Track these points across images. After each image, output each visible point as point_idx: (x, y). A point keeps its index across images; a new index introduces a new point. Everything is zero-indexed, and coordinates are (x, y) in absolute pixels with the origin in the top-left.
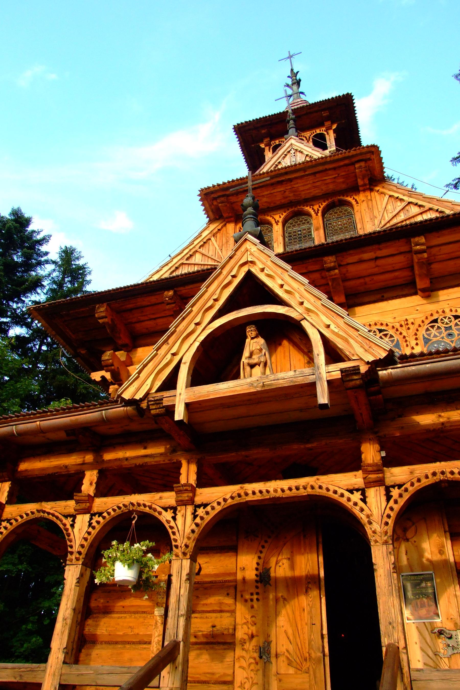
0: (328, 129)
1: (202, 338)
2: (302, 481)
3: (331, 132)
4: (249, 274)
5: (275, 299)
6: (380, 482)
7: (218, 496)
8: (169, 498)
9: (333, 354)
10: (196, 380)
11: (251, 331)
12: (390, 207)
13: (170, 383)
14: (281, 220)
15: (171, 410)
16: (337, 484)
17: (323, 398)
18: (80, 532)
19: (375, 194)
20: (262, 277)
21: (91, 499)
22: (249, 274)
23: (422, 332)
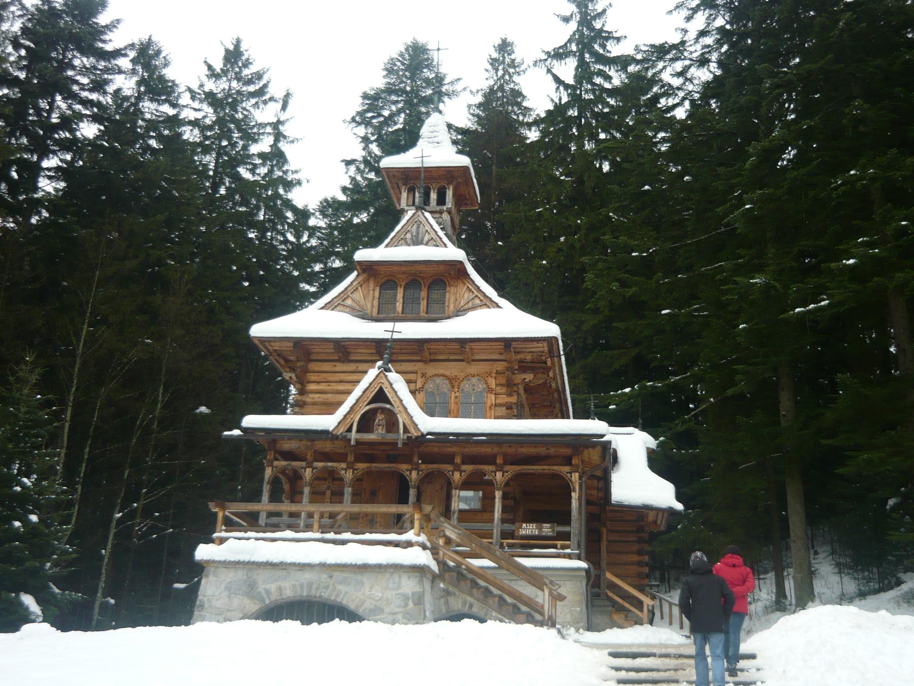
0: (449, 184)
1: (362, 412)
2: (391, 465)
3: (451, 187)
4: (381, 389)
5: (390, 403)
6: (416, 469)
7: (362, 466)
8: (344, 465)
9: (406, 430)
10: (358, 431)
11: (380, 411)
12: (466, 296)
13: (349, 430)
14: (403, 284)
15: (350, 440)
16: (404, 467)
17: (400, 445)
18: (308, 473)
19: (460, 281)
20: (386, 390)
21: (312, 462)
22: (381, 389)
23: (462, 385)
